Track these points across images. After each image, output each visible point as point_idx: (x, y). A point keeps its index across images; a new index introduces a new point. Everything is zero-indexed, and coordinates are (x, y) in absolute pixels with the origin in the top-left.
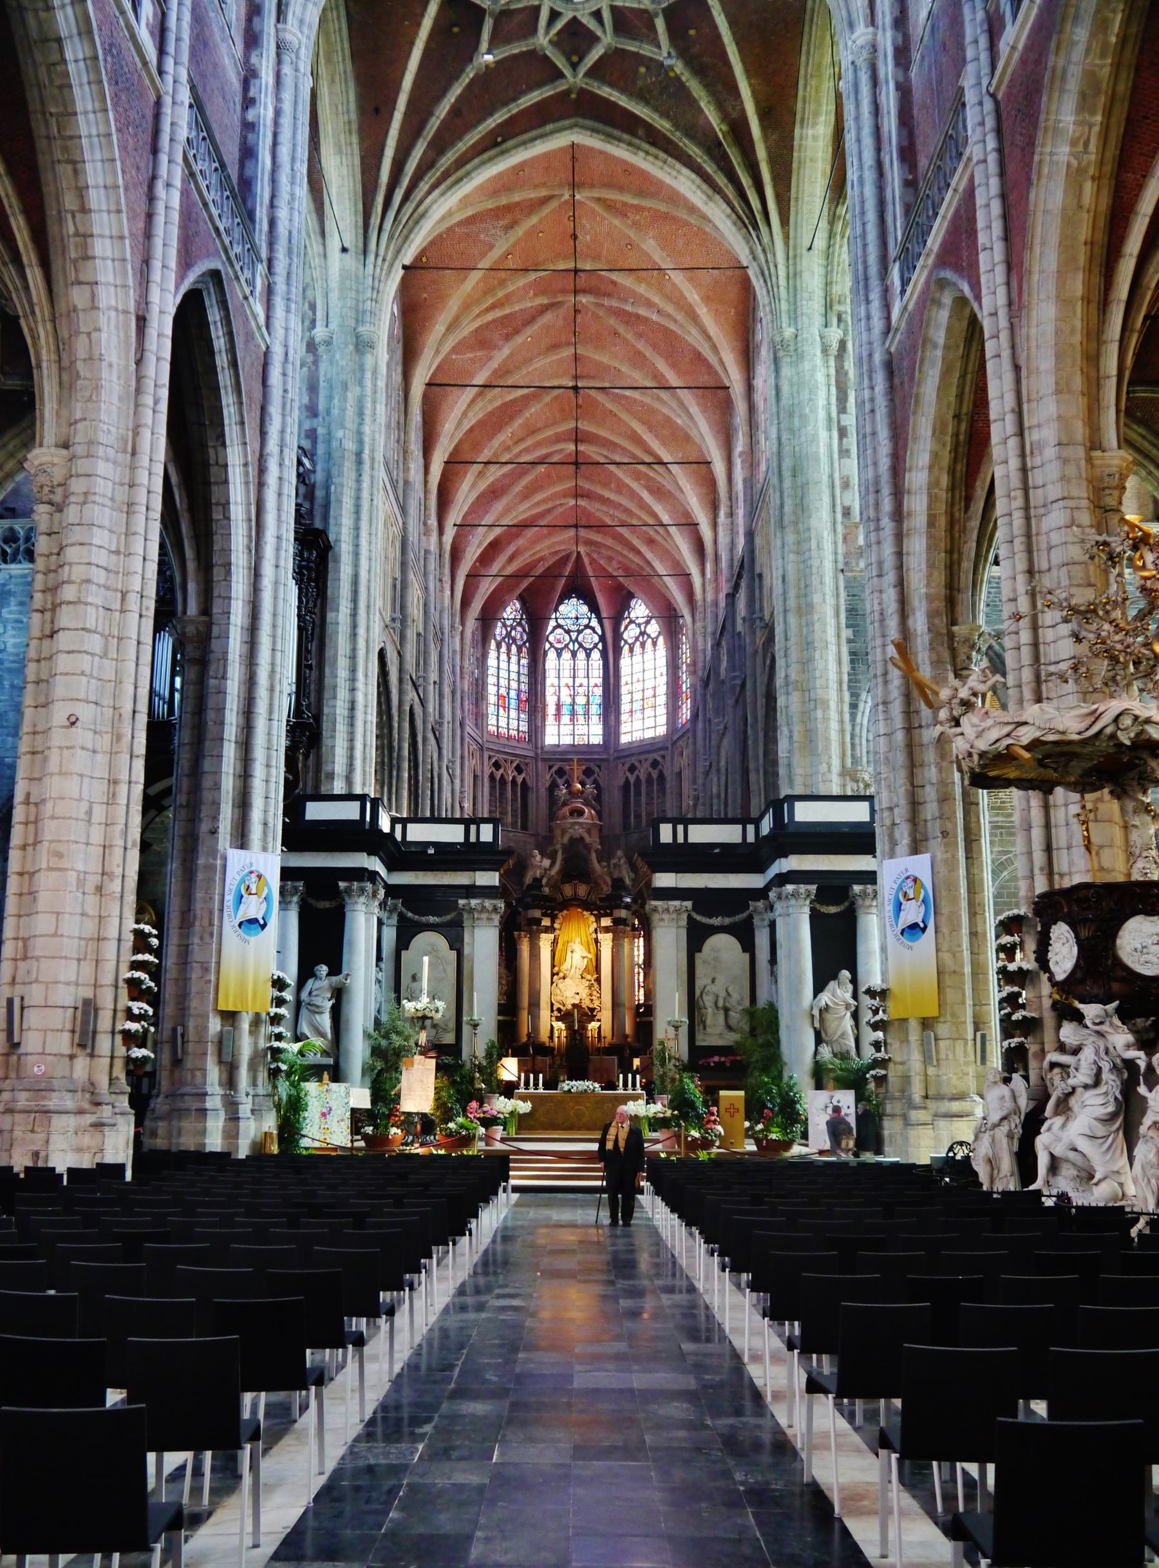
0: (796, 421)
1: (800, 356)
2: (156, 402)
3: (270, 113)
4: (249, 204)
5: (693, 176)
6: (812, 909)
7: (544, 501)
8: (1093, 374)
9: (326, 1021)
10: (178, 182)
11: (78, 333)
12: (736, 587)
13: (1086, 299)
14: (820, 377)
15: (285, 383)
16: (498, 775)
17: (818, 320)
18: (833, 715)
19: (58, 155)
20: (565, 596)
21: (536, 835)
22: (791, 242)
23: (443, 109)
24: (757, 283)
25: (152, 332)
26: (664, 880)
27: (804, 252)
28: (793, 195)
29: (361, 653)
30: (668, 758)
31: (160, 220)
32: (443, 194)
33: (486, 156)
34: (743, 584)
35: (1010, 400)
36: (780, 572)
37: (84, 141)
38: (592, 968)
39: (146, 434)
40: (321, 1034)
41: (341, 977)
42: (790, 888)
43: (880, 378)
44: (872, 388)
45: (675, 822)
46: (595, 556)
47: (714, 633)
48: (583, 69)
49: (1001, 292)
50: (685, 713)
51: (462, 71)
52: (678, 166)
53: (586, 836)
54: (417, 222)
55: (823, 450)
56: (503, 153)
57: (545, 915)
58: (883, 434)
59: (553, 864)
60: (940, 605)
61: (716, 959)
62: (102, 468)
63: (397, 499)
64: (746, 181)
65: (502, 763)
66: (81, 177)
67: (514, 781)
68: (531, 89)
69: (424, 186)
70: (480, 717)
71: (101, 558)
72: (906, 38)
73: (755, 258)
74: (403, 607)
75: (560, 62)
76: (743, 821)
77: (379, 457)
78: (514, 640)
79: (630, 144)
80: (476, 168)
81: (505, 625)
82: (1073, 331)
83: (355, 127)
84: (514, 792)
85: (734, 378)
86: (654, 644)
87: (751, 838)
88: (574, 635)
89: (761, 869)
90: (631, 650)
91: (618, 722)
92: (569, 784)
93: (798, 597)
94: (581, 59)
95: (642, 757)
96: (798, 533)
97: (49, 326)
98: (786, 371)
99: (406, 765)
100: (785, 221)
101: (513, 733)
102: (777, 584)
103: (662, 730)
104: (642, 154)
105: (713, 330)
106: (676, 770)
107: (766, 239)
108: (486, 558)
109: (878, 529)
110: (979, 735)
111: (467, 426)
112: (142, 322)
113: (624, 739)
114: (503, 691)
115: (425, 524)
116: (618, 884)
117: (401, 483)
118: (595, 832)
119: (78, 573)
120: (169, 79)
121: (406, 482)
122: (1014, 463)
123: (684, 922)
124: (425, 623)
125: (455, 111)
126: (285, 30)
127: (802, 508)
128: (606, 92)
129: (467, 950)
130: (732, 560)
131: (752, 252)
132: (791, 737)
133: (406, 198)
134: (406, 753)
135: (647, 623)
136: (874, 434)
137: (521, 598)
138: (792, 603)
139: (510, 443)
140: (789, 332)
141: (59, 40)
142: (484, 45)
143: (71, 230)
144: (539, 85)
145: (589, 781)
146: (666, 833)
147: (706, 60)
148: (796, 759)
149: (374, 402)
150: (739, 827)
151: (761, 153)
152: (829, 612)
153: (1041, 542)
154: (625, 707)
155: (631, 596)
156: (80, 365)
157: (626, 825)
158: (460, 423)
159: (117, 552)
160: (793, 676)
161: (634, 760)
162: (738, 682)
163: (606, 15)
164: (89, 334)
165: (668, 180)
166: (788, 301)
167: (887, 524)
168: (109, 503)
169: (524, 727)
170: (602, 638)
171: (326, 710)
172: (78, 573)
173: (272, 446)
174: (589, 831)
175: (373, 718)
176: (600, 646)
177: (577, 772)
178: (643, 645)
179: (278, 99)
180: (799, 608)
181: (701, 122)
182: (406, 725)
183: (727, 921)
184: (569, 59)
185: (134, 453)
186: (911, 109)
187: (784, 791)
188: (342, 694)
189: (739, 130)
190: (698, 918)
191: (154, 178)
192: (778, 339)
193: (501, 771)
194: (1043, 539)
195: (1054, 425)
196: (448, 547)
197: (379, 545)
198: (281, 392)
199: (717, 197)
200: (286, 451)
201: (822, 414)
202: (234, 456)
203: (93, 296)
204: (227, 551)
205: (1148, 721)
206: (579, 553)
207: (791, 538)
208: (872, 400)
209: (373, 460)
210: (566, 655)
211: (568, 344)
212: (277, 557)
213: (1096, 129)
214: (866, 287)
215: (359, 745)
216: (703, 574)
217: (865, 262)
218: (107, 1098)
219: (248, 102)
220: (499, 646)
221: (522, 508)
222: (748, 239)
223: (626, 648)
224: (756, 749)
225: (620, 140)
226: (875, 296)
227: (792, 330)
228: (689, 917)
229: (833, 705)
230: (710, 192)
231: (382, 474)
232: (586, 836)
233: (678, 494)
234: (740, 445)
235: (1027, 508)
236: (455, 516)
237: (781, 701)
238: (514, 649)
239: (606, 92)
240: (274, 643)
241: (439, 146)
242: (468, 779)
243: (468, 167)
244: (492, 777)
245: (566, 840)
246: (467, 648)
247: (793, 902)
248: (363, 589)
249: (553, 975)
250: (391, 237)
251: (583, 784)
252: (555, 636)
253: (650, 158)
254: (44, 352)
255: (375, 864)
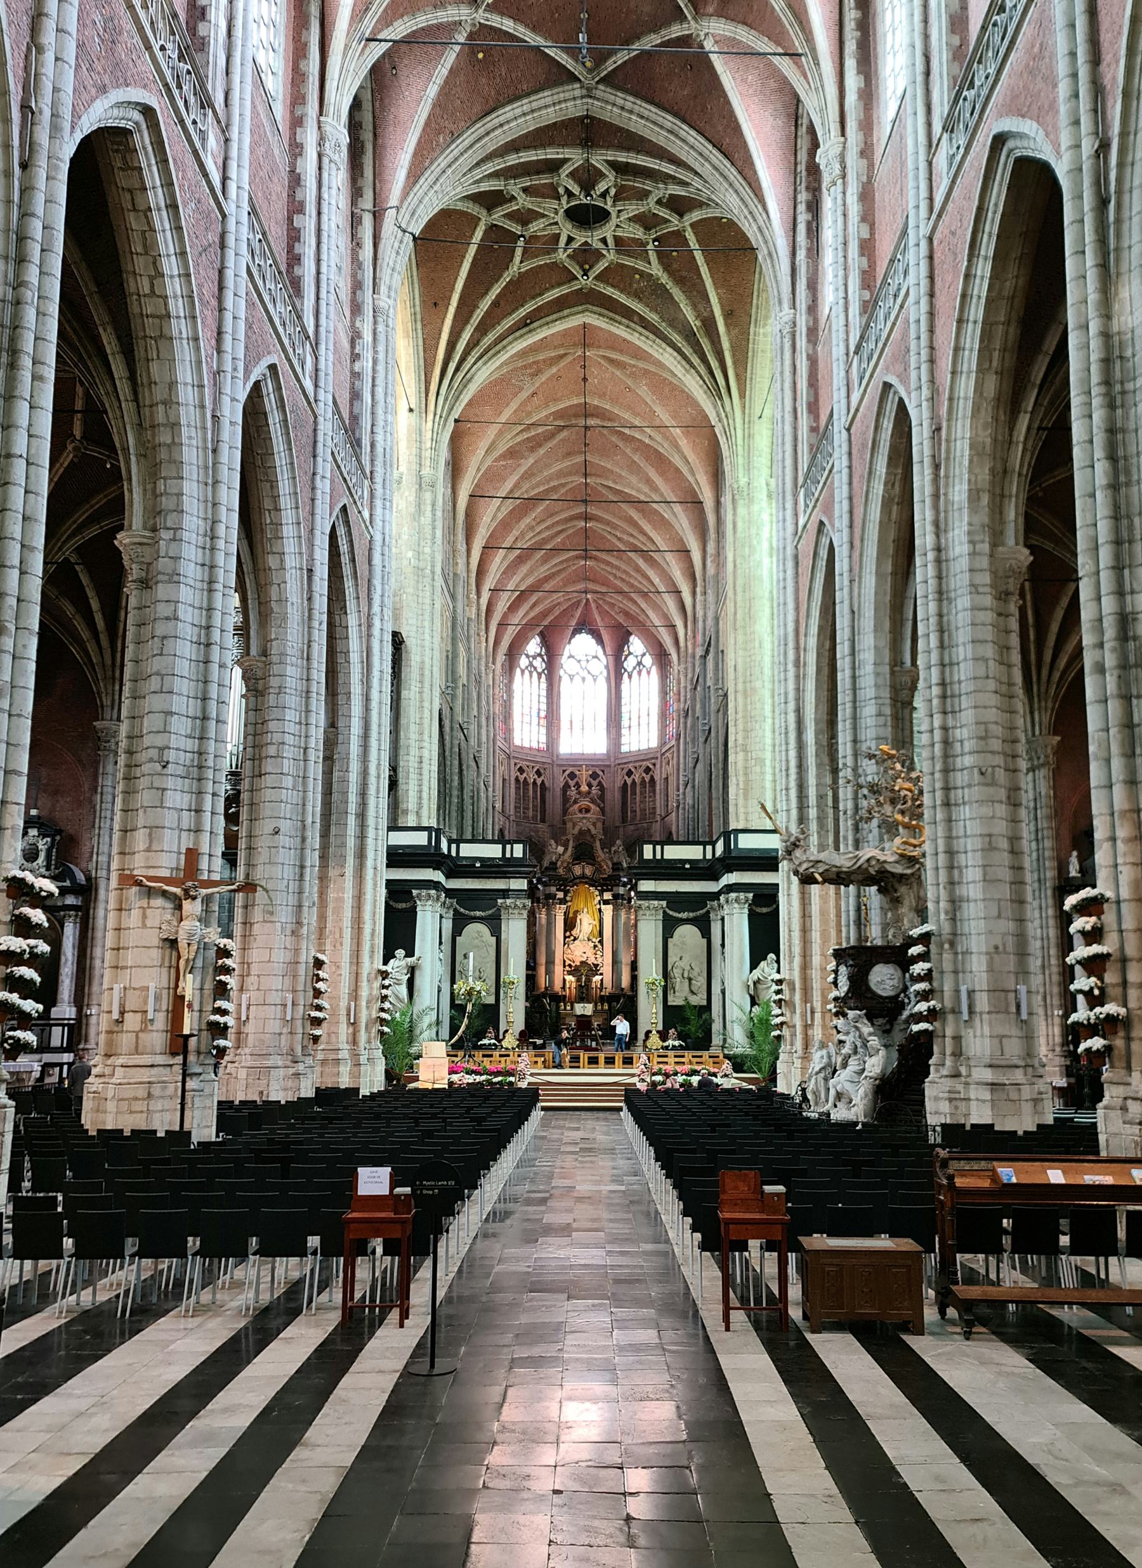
0: (747, 550)
1: (751, 500)
2: (320, 624)
3: (370, 364)
4: (357, 435)
5: (675, 354)
6: (749, 910)
7: (562, 562)
8: (898, 617)
9: (403, 991)
10: (328, 475)
11: (271, 584)
12: (707, 652)
13: (894, 574)
14: (765, 517)
15: (383, 561)
16: (521, 778)
17: (766, 471)
18: (768, 769)
19: (261, 476)
20: (577, 631)
21: (551, 826)
22: (747, 411)
23: (485, 304)
24: (722, 440)
25: (316, 579)
26: (646, 886)
27: (756, 419)
28: (749, 376)
29: (426, 721)
30: (658, 766)
31: (318, 503)
32: (485, 364)
33: (518, 334)
34: (712, 649)
35: (847, 631)
36: (733, 663)
37: (278, 469)
38: (596, 932)
39: (315, 646)
40: (401, 1001)
41: (414, 959)
42: (733, 895)
43: (790, 564)
44: (785, 572)
45: (655, 843)
46: (601, 602)
47: (692, 680)
48: (593, 274)
49: (846, 561)
50: (672, 729)
51: (500, 276)
52: (664, 345)
53: (591, 827)
54: (465, 386)
55: (765, 573)
56: (530, 331)
57: (558, 890)
58: (791, 605)
59: (566, 849)
60: (824, 726)
61: (683, 943)
62: (290, 671)
63: (449, 591)
64: (714, 364)
65: (525, 768)
66: (275, 490)
67: (535, 783)
68: (553, 287)
69: (471, 360)
70: (508, 731)
71: (291, 728)
72: (816, 321)
73: (720, 421)
74: (454, 672)
75: (576, 271)
76: (704, 844)
77: (438, 570)
78: (535, 668)
79: (628, 327)
80: (511, 343)
81: (528, 656)
82: (885, 594)
83: (419, 317)
84: (535, 792)
85: (707, 495)
86: (649, 673)
87: (709, 856)
88: (584, 664)
89: (716, 878)
90: (630, 677)
91: (619, 735)
92: (578, 785)
93: (744, 682)
94: (591, 267)
95: (637, 764)
96: (746, 634)
97: (252, 576)
98: (742, 511)
99: (455, 793)
100: (742, 395)
101: (535, 745)
102: (731, 670)
103: (654, 743)
104: (637, 335)
105: (692, 457)
106: (664, 776)
107: (728, 408)
108: (513, 608)
109: (786, 671)
110: (800, 864)
111: (500, 516)
112: (310, 571)
113: (624, 749)
114: (526, 710)
115: (468, 598)
116: (617, 867)
117: (451, 575)
118: (599, 825)
119: (277, 737)
120: (321, 404)
121: (455, 574)
122: (848, 673)
123: (661, 917)
124: (468, 676)
125: (495, 304)
126: (379, 299)
127: (750, 616)
128: (609, 291)
129: (503, 937)
130: (705, 629)
131: (718, 415)
132: (738, 784)
133: (457, 369)
134: (456, 783)
135: (643, 655)
136: (785, 604)
137: (542, 635)
138: (740, 687)
139: (534, 524)
140: (743, 481)
141: (265, 414)
142: (517, 258)
143: (268, 521)
144: (559, 285)
145: (595, 783)
146: (648, 852)
147: (684, 274)
148: (741, 802)
149: (434, 528)
150: (701, 847)
151: (726, 345)
152: (767, 694)
153: (862, 723)
154: (625, 723)
155: (630, 634)
156: (273, 604)
157: (624, 819)
158: (495, 516)
159: (300, 723)
160: (740, 741)
161: (630, 766)
162: (707, 728)
163: (610, 241)
164: (279, 585)
165: (656, 355)
166: (743, 456)
167: (790, 666)
168: (294, 692)
169: (543, 739)
170: (607, 667)
171: (401, 764)
172: (277, 737)
173: (376, 609)
174: (594, 824)
175: (435, 768)
176: (605, 673)
177: (584, 775)
178: (640, 673)
179: (376, 352)
180: (745, 691)
181: (682, 317)
182: (456, 762)
183: (691, 915)
184: (581, 267)
185: (308, 659)
186: (817, 374)
187: (733, 826)
188: (414, 751)
189: (709, 325)
190: (671, 913)
191: (314, 474)
192: (735, 486)
193: (525, 775)
194: (863, 721)
195: (872, 652)
196: (484, 608)
197: (437, 640)
198: (381, 568)
199: (693, 371)
200: (385, 609)
201: (765, 546)
202: (352, 620)
203: (282, 561)
204: (348, 684)
205: (885, 862)
206: (587, 600)
207: (740, 638)
208: (785, 579)
209: (433, 573)
210: (577, 679)
211: (580, 452)
212: (381, 685)
213: (899, 477)
214: (784, 497)
215: (425, 789)
216: (686, 626)
217: (783, 480)
218: (301, 1058)
219: (355, 357)
220: (523, 672)
221: (542, 569)
222: (715, 407)
223: (626, 675)
224: (717, 783)
225: (620, 323)
226: (789, 505)
227: (746, 479)
228: (664, 912)
229: (768, 763)
230: (688, 367)
231: (439, 581)
232: (591, 827)
233: (665, 566)
234: (711, 548)
235: (854, 701)
236: (489, 583)
237: (731, 759)
238: (535, 674)
239: (609, 291)
240: (380, 745)
241: (483, 329)
242: (499, 783)
243: (504, 342)
244: (517, 779)
245: (576, 831)
246: (497, 678)
247: (736, 905)
248: (427, 673)
249: (565, 937)
250: (446, 399)
251: (590, 785)
252: (567, 665)
253: (642, 338)
254: (249, 593)
255: (438, 876)
